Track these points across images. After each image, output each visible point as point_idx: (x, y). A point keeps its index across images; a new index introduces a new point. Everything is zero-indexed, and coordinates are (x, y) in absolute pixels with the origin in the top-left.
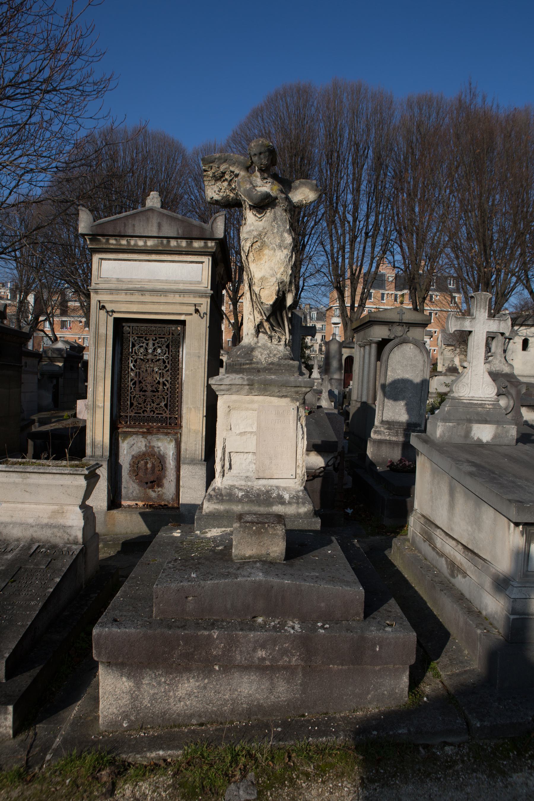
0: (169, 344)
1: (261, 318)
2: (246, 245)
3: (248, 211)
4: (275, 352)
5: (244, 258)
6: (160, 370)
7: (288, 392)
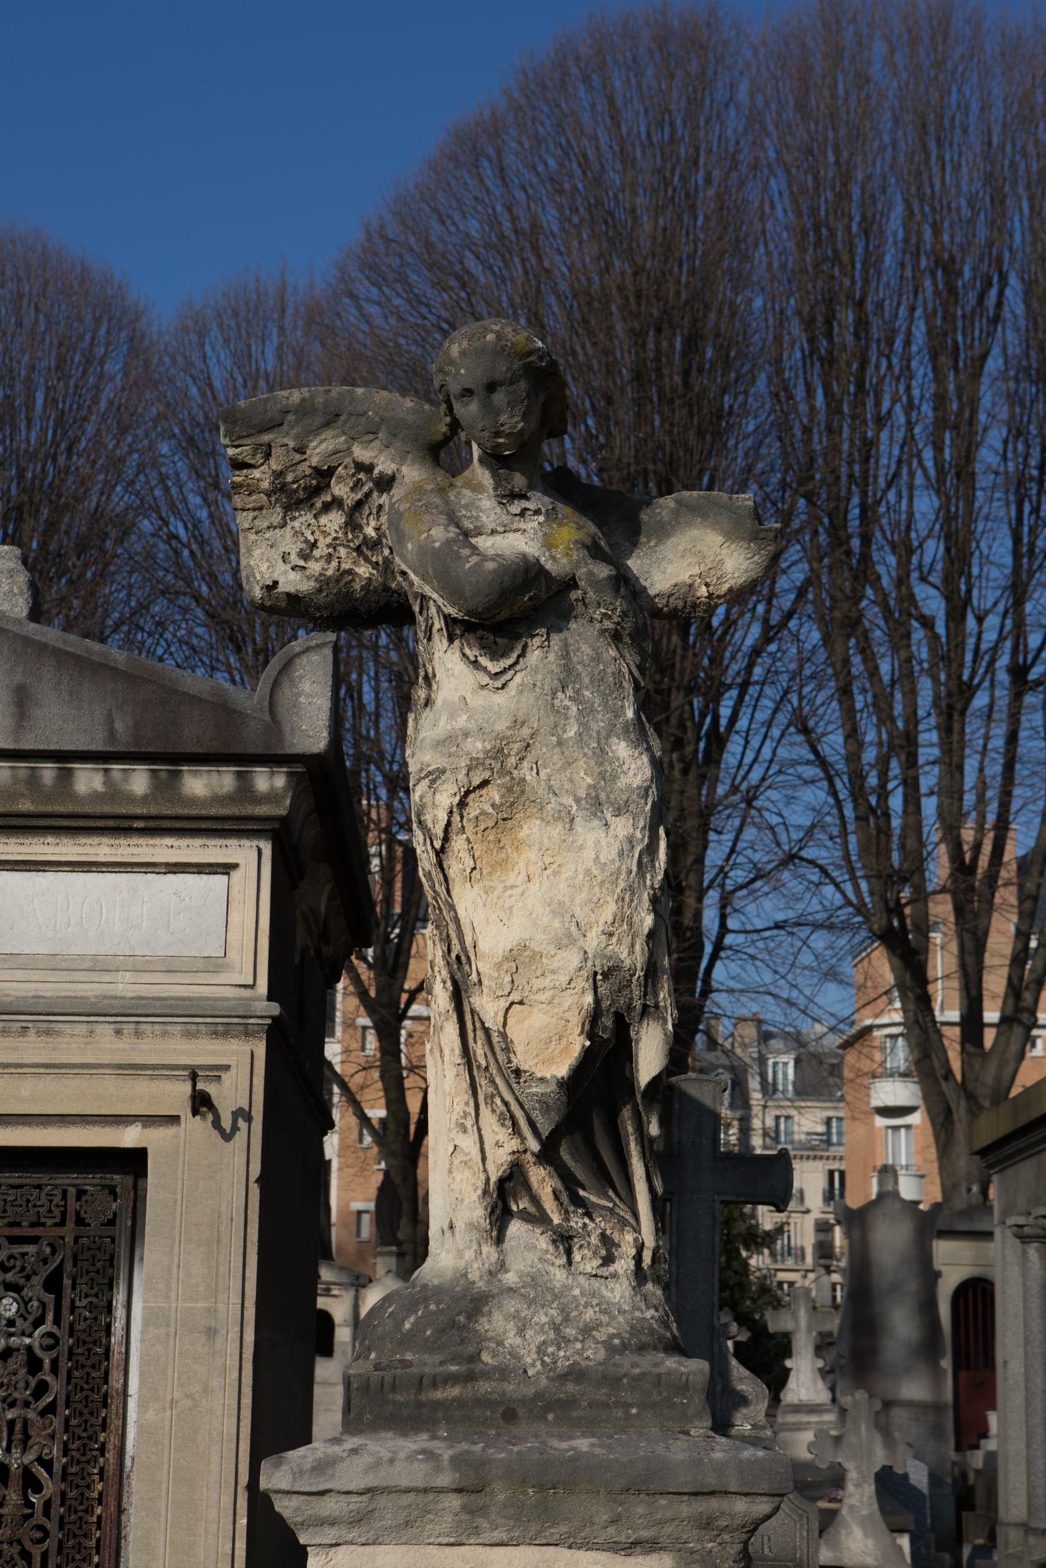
0: (60, 1269)
1: (514, 1144)
2: (435, 803)
3: (440, 643)
4: (589, 1314)
5: (426, 861)
6: (12, 1405)
7: (661, 1523)
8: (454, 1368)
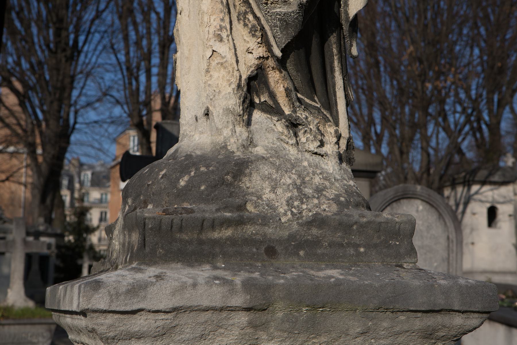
1: (261, 51)
4: (317, 180)
7: (399, 334)
8: (228, 214)
